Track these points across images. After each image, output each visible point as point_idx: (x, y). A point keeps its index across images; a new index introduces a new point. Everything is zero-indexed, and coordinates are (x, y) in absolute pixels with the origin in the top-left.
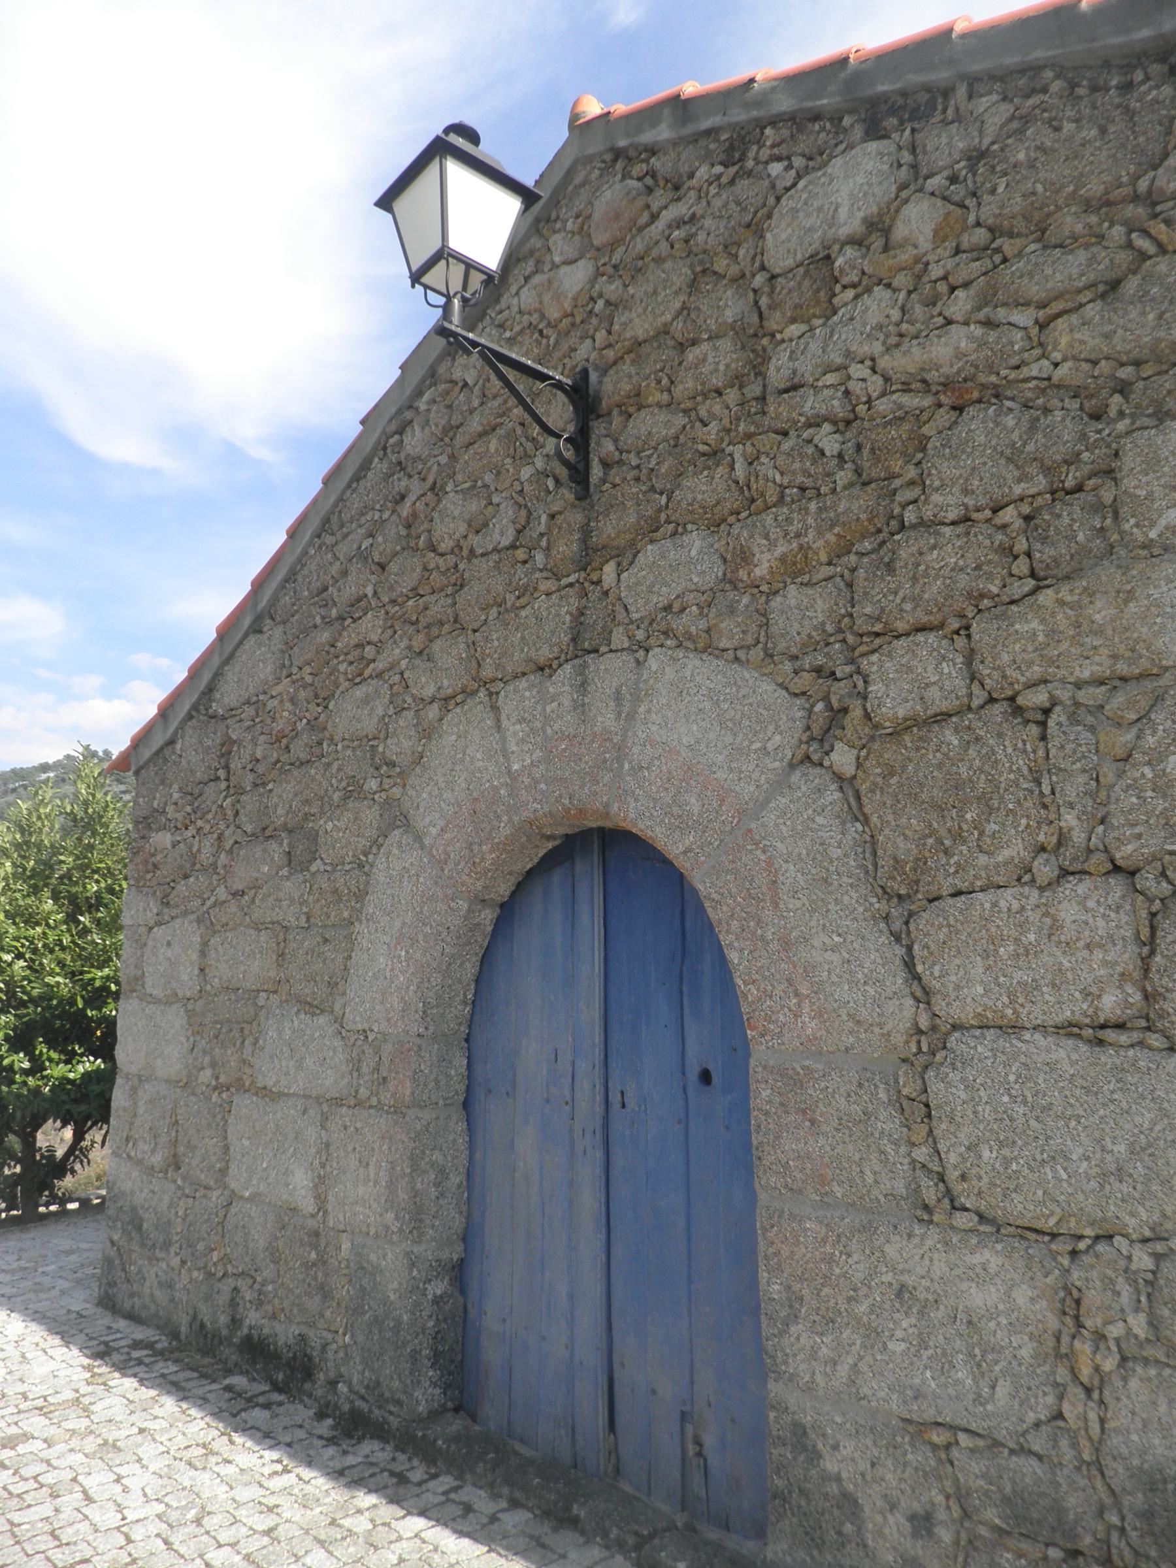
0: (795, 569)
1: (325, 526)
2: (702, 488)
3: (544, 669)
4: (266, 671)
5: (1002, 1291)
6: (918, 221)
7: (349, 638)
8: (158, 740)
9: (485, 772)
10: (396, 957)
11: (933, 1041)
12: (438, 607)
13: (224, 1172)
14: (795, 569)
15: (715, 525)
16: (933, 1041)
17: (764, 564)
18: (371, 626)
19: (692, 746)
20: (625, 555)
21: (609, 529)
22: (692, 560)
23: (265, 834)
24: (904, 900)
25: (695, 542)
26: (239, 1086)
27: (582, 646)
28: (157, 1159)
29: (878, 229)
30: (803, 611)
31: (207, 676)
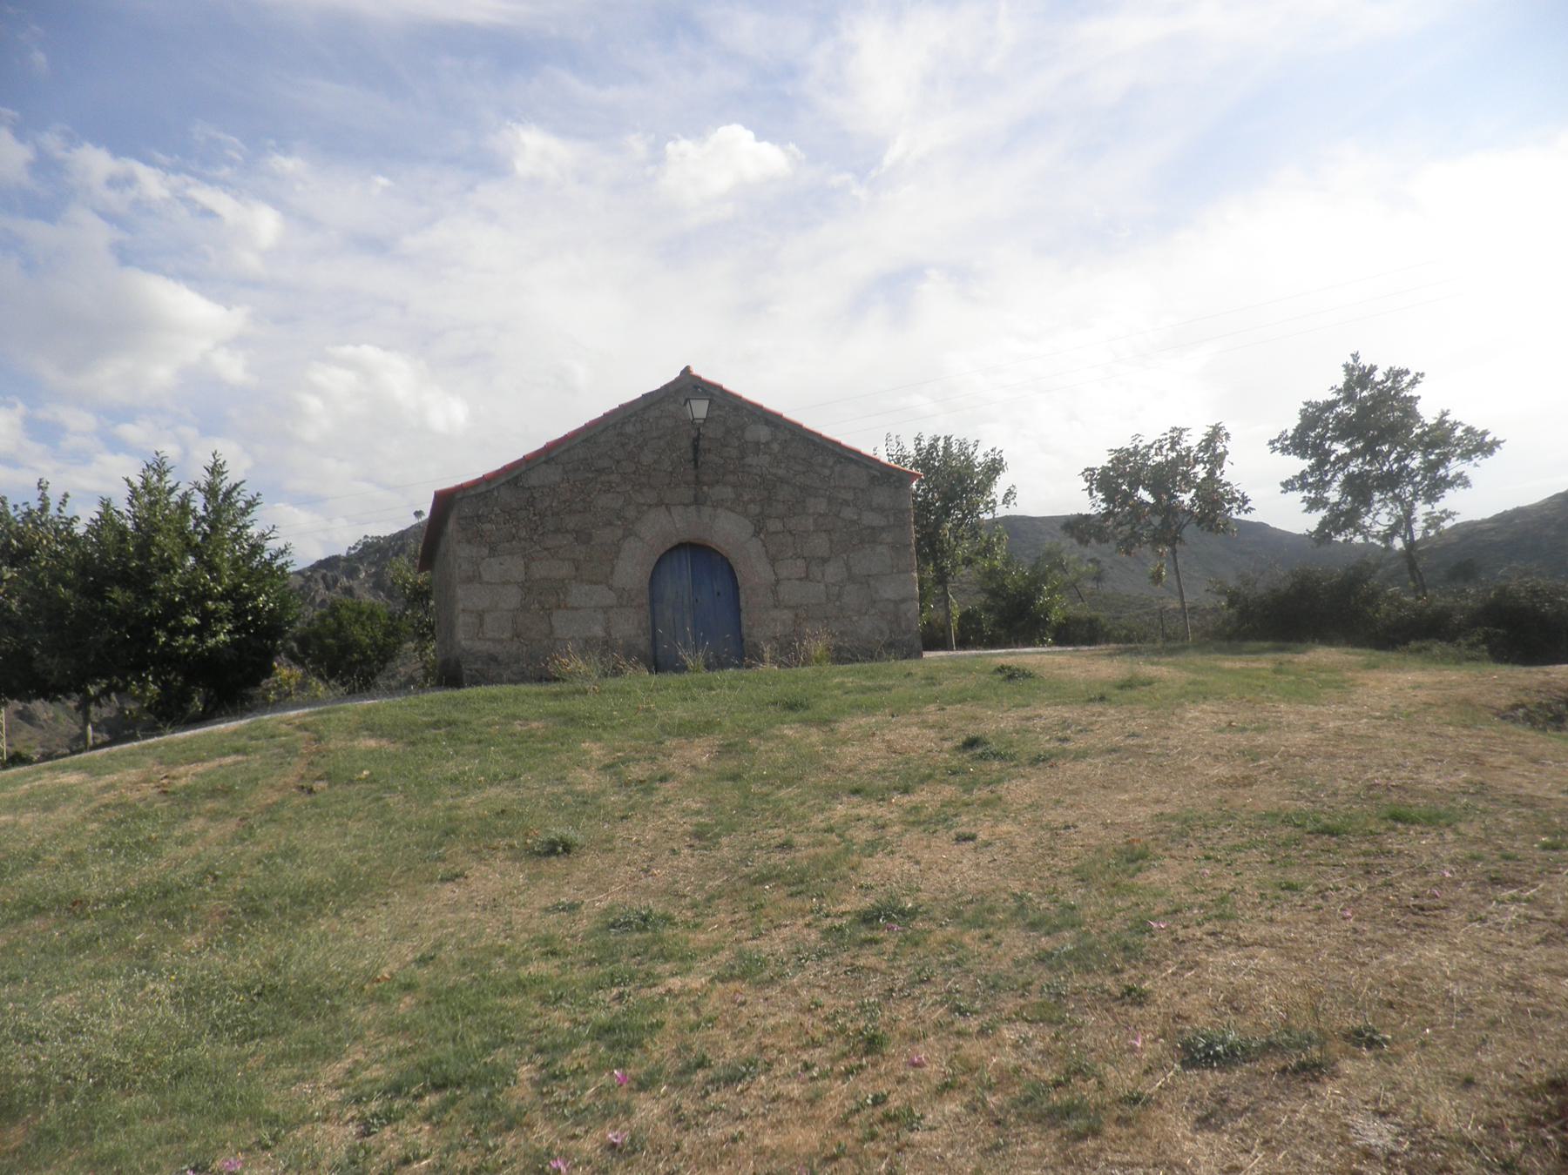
0: (752, 501)
1: (586, 440)
2: (731, 478)
3: (687, 505)
4: (558, 479)
5: (787, 615)
6: (776, 447)
7: (604, 478)
8: (483, 489)
9: (666, 525)
10: (632, 570)
11: (778, 581)
12: (643, 479)
13: (552, 632)
14: (752, 501)
15: (734, 486)
16: (778, 581)
17: (746, 498)
18: (615, 478)
19: (727, 530)
20: (711, 485)
21: (706, 479)
22: (728, 492)
23: (557, 531)
24: (773, 561)
25: (730, 489)
26: (559, 607)
27: (698, 501)
28: (506, 635)
29: (767, 444)
30: (754, 509)
31: (516, 473)
